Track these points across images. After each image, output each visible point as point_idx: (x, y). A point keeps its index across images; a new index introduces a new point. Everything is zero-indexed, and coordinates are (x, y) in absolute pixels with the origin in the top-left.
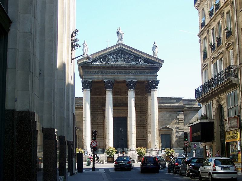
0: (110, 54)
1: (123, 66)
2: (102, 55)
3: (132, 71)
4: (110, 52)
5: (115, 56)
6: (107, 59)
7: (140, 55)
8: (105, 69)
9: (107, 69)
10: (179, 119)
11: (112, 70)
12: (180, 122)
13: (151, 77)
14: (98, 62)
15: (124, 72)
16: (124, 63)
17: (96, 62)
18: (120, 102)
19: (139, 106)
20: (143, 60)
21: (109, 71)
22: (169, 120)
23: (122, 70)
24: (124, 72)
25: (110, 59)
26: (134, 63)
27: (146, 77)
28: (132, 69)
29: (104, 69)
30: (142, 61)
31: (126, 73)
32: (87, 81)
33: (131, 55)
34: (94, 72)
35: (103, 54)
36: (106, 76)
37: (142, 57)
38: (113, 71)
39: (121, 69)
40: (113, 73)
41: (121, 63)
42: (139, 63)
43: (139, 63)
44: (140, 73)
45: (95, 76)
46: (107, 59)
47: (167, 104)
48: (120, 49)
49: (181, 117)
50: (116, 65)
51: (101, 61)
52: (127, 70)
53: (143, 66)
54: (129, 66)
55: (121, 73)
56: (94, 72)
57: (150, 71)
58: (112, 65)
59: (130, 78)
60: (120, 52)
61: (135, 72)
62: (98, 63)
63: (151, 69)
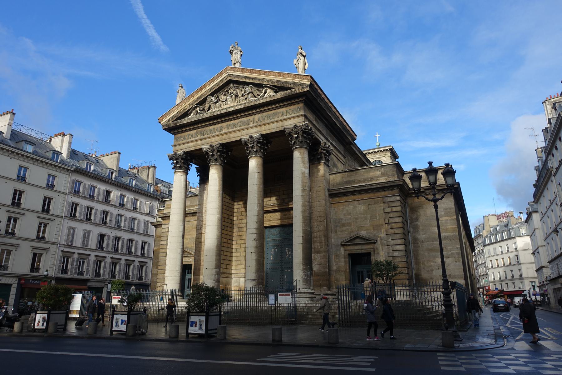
0: (212, 94)
1: (232, 109)
2: (198, 98)
4: (211, 89)
5: (222, 97)
6: (207, 106)
7: (263, 80)
9: (210, 125)
10: (392, 215)
11: (219, 126)
12: (392, 220)
14: (192, 114)
15: (239, 124)
17: (189, 114)
20: (270, 88)
22: (366, 219)
23: (238, 121)
24: (239, 124)
26: (252, 100)
27: (280, 124)
29: (204, 126)
30: (269, 90)
31: (243, 123)
32: (176, 154)
33: (248, 84)
34: (190, 137)
35: (201, 97)
36: (207, 138)
37: (267, 80)
38: (220, 127)
39: (234, 119)
40: (221, 129)
42: (263, 96)
43: (263, 96)
44: (268, 117)
45: (191, 142)
46: (207, 106)
47: (359, 183)
48: (229, 78)
49: (394, 209)
50: (220, 111)
51: (198, 113)
52: (245, 119)
54: (243, 107)
55: (234, 126)
56: (190, 137)
57: (288, 109)
59: (250, 130)
60: (232, 85)
61: (259, 120)
63: (291, 104)
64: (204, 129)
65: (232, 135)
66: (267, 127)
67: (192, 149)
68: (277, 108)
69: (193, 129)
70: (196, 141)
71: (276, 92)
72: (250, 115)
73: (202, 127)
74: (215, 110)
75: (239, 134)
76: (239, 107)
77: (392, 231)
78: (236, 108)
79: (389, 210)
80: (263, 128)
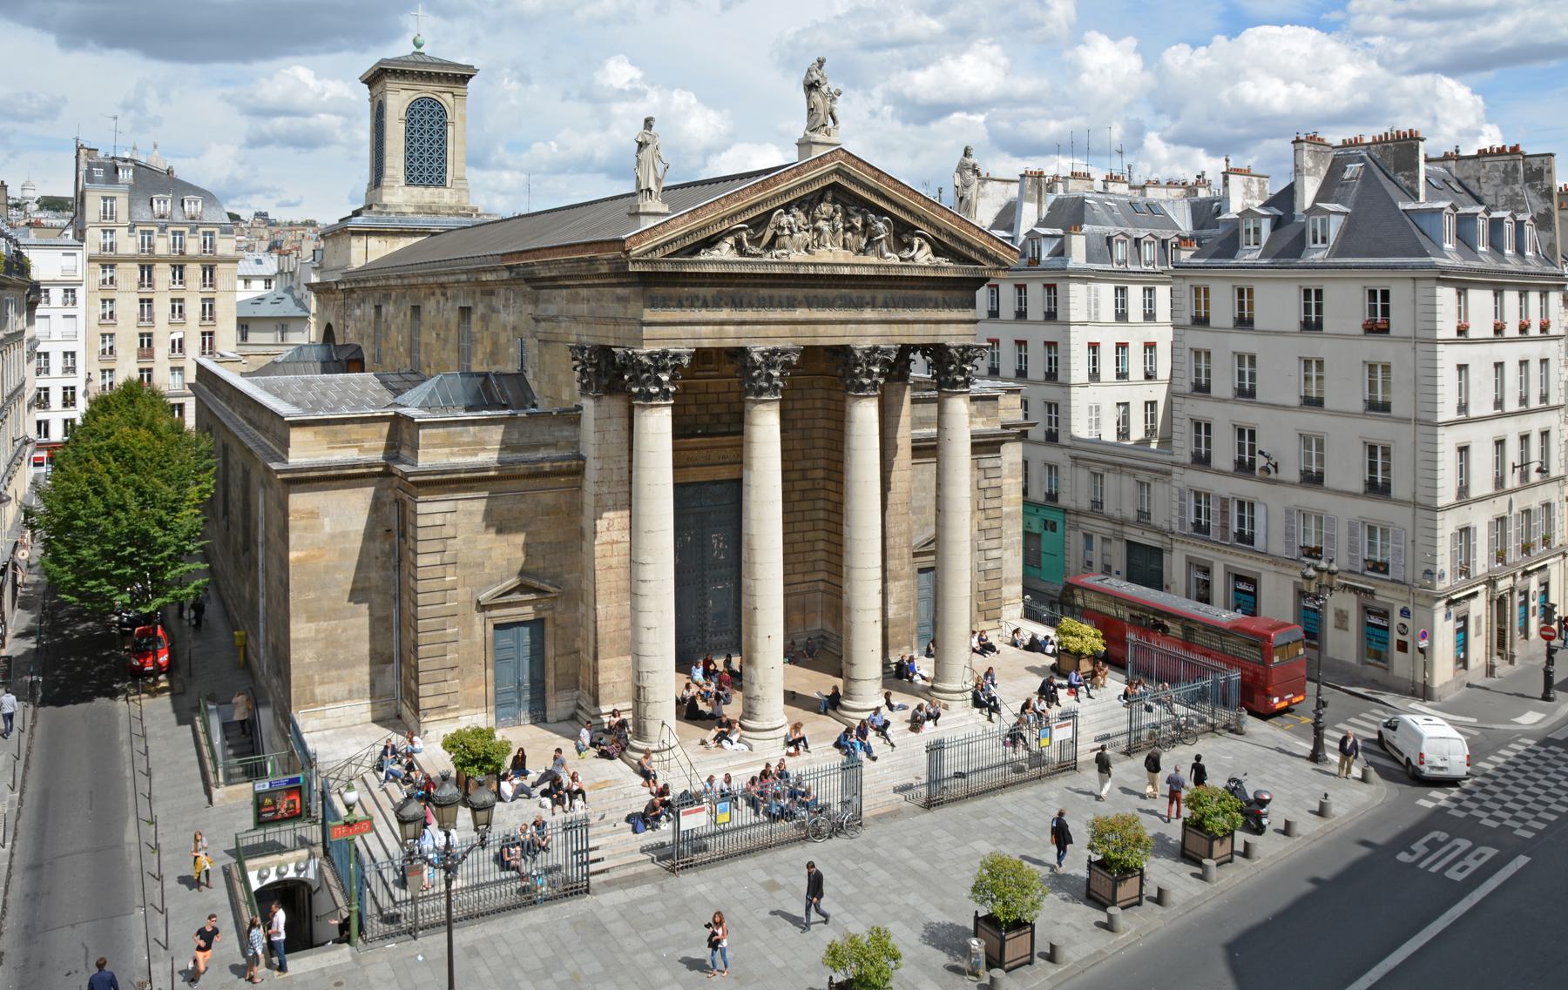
1: (846, 271)
3: (874, 298)
6: (769, 234)
8: (755, 285)
9: (764, 286)
12: (990, 504)
13: (953, 329)
16: (851, 257)
18: (717, 409)
19: (799, 424)
21: (771, 298)
25: (787, 232)
28: (876, 287)
29: (746, 285)
41: (834, 255)
53: (931, 273)
54: (872, 272)
58: (797, 264)
62: (725, 252)
64: (743, 291)
65: (821, 329)
66: (904, 328)
67: (706, 344)
68: (927, 288)
69: (711, 285)
70: (722, 323)
71: (936, 253)
72: (868, 287)
73: (738, 285)
74: (794, 255)
75: (838, 329)
76: (865, 272)
77: (986, 524)
78: (857, 271)
79: (984, 484)
80: (895, 329)
